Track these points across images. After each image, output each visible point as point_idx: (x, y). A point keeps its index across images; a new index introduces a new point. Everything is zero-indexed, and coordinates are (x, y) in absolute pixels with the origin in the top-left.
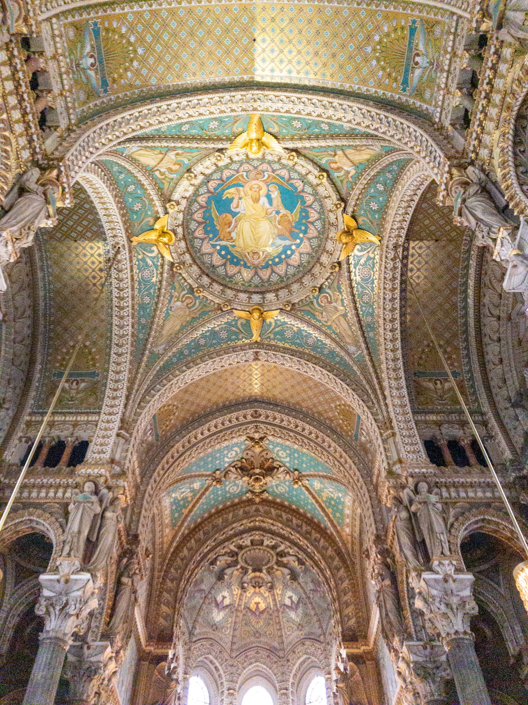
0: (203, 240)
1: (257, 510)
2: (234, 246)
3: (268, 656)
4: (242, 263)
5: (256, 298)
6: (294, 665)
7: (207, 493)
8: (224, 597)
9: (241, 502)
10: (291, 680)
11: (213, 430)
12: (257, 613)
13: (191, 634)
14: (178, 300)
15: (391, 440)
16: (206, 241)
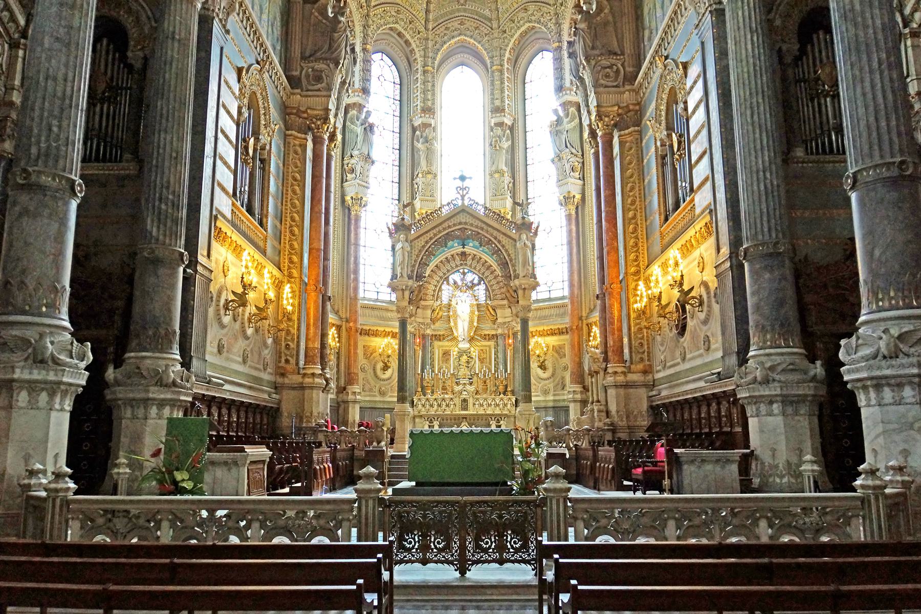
3: (476, 28)
6: (512, 36)
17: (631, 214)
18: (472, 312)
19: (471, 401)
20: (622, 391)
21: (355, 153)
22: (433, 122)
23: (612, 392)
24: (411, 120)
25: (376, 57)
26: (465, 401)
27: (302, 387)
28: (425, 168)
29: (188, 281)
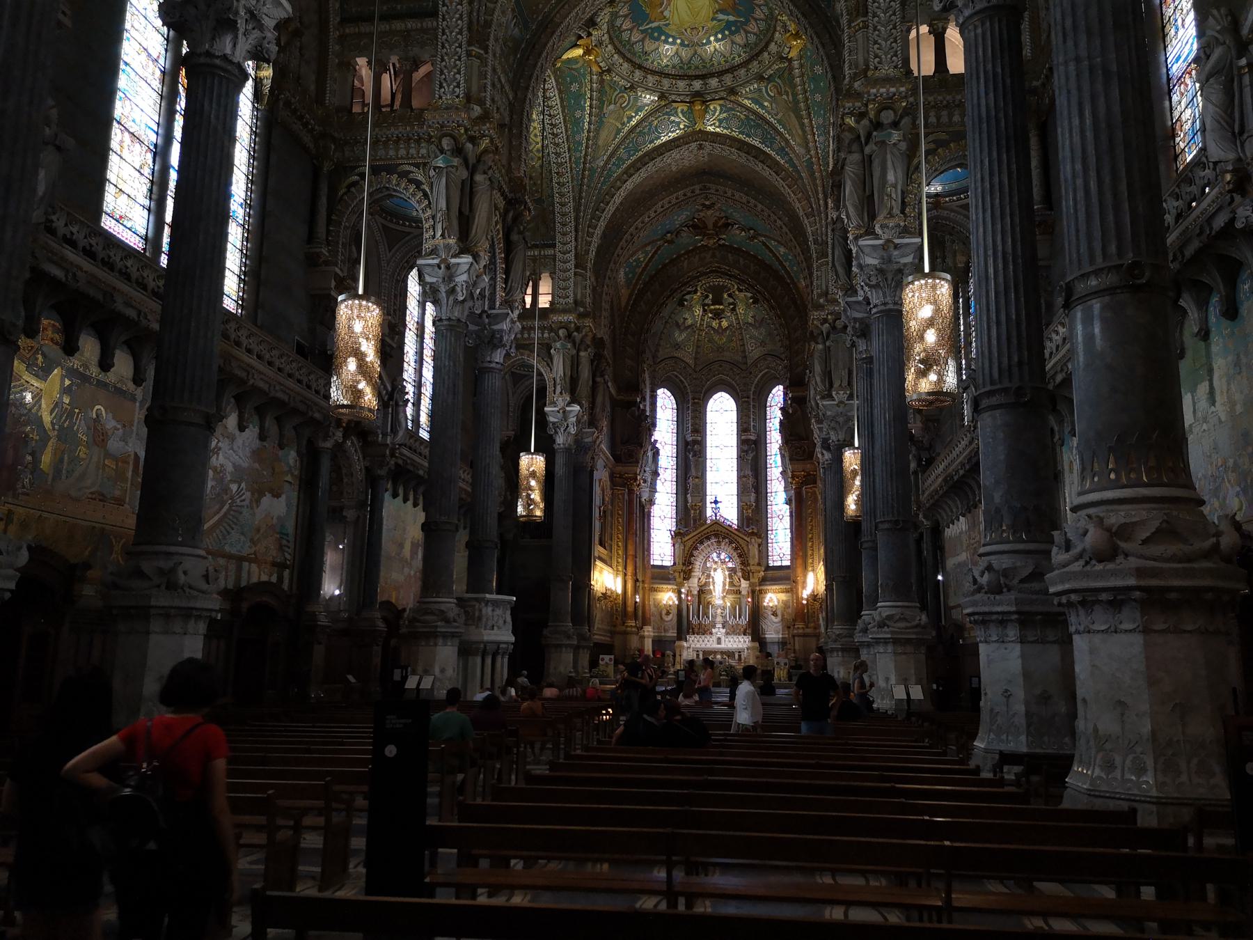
0: (631, 30)
1: (714, 256)
2: (667, 25)
4: (679, 41)
5: (697, 85)
6: (756, 377)
7: (659, 252)
8: (685, 319)
9: (696, 248)
10: (753, 389)
11: (660, 210)
12: (720, 331)
13: (654, 357)
14: (610, 103)
15: (823, 269)
16: (635, 30)
17: (810, 536)
18: (725, 579)
19: (723, 639)
20: (802, 638)
21: (647, 469)
22: (699, 438)
23: (796, 638)
24: (685, 437)
25: (660, 392)
26: (719, 639)
27: (625, 633)
28: (694, 474)
29: (589, 592)
